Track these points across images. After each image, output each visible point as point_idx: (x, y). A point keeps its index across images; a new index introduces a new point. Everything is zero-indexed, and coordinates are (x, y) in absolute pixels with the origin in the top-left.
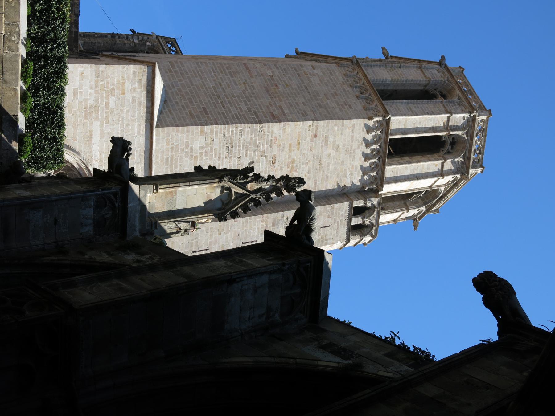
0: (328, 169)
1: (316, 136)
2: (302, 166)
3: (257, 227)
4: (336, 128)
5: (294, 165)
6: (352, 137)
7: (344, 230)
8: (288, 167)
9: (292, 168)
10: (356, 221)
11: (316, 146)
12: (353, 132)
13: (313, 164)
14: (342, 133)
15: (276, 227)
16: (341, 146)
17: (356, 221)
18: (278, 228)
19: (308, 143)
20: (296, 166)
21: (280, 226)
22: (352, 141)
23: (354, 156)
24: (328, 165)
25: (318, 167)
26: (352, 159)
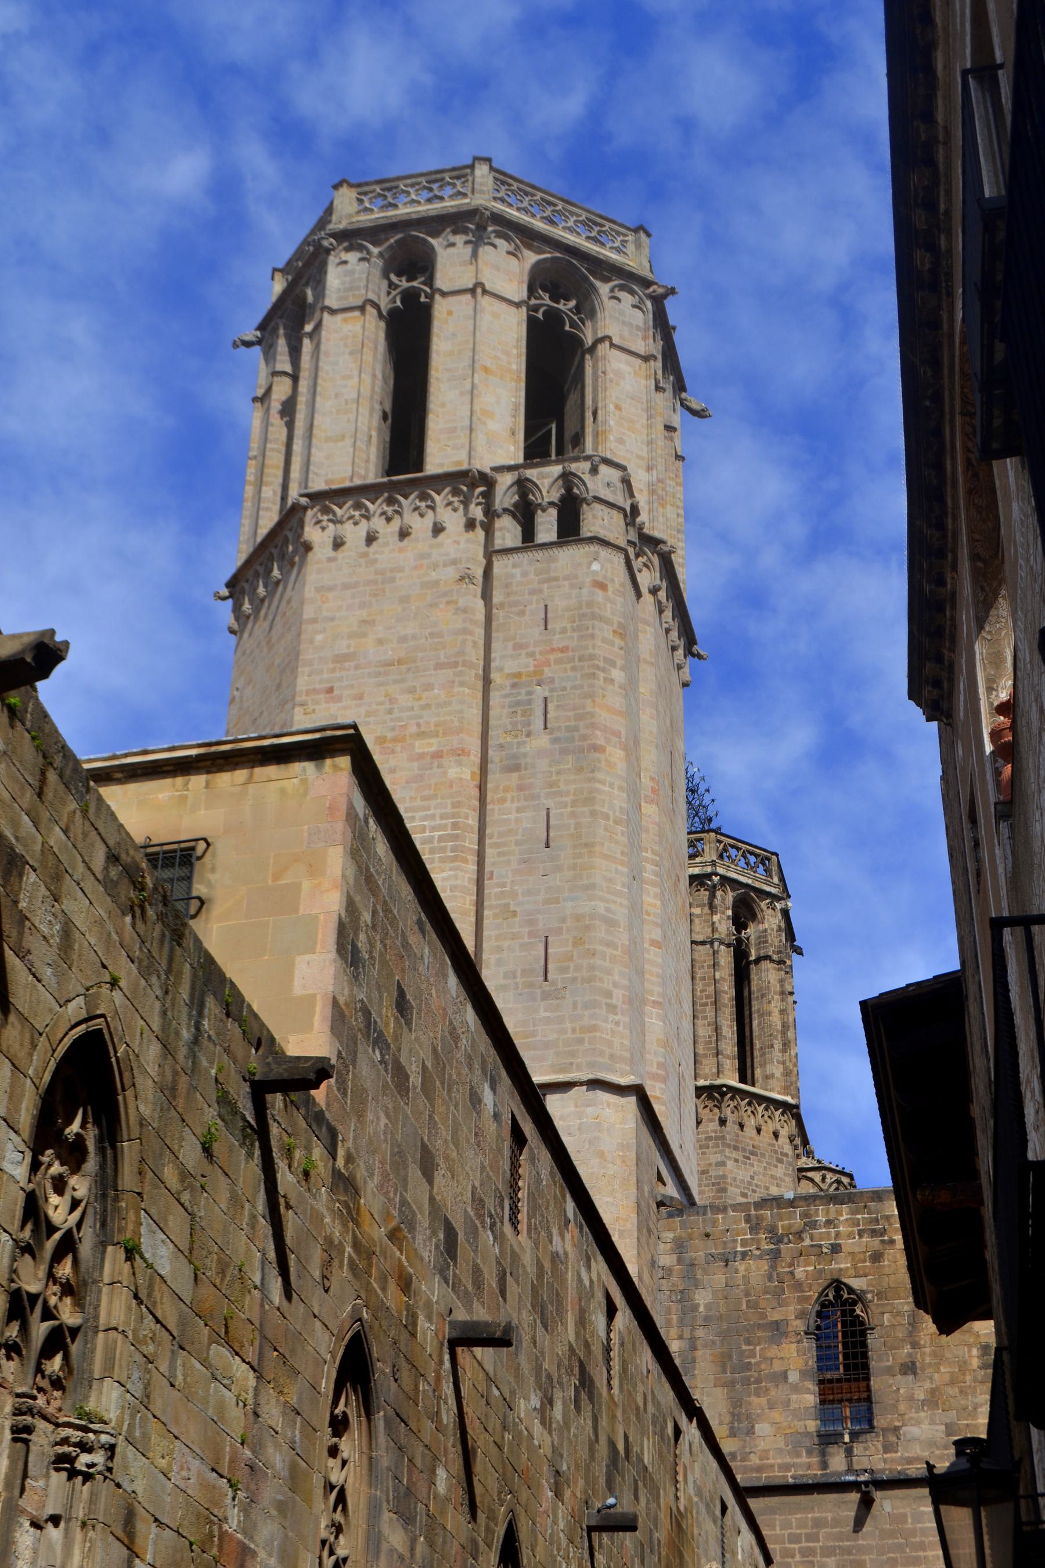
0: (414, 637)
1: (330, 690)
2: (396, 714)
3: (513, 816)
4: (319, 638)
5: (389, 735)
6: (346, 586)
7: (568, 556)
8: (393, 752)
9: (395, 740)
10: (547, 526)
11: (352, 686)
12: (331, 589)
13: (395, 682)
14: (332, 619)
15: (522, 761)
16: (363, 614)
17: (547, 526)
18: (525, 755)
19: (345, 708)
20: (393, 729)
21: (522, 750)
22: (356, 585)
23: (392, 570)
24: (402, 639)
25: (404, 668)
26: (398, 575)
